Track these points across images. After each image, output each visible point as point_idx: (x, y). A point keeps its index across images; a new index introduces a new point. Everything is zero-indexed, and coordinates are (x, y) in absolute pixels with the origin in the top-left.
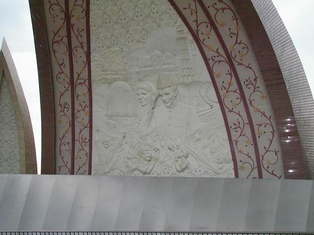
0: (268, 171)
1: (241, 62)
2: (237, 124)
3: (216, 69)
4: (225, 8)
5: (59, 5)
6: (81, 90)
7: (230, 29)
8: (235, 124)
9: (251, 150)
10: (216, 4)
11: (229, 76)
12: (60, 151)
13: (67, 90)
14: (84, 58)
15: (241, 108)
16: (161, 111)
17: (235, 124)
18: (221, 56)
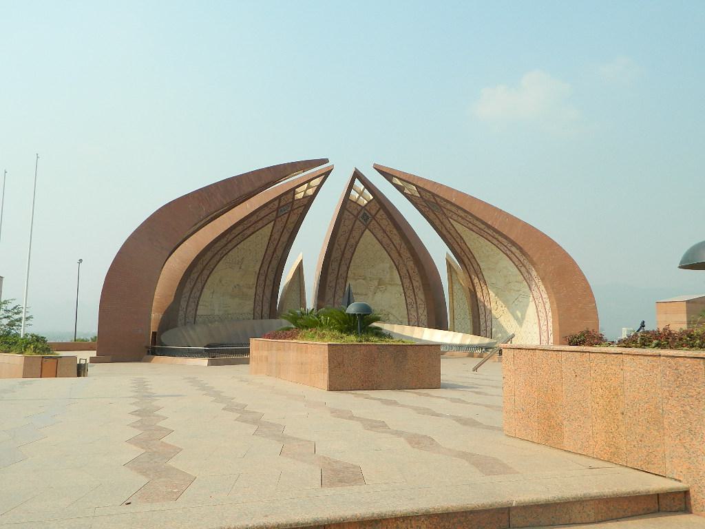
3: (404, 281)
6: (341, 281)
9: (415, 314)
14: (346, 269)
15: (413, 297)
16: (379, 295)
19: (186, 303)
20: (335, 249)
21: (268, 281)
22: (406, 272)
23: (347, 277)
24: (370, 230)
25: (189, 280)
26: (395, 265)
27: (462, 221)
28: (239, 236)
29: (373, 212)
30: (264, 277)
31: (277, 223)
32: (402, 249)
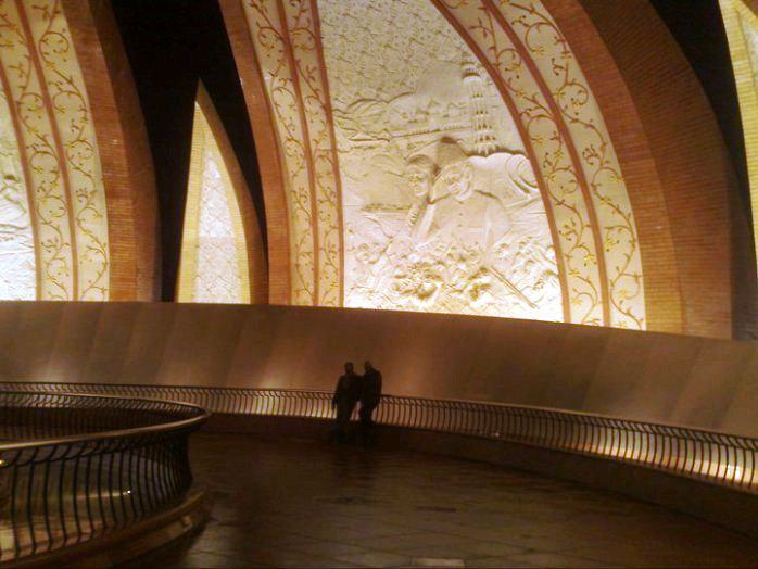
0: (620, 310)
1: (576, 117)
2: (571, 225)
4: (542, 23)
5: (272, 28)
6: (322, 167)
7: (553, 59)
8: (566, 226)
10: (524, 17)
11: (556, 142)
12: (297, 265)
13: (301, 168)
15: (576, 198)
17: (566, 226)
18: (542, 107)
20: (255, 30)
21: (73, 173)
22: (533, 89)
26: (485, 63)
30: (51, 162)
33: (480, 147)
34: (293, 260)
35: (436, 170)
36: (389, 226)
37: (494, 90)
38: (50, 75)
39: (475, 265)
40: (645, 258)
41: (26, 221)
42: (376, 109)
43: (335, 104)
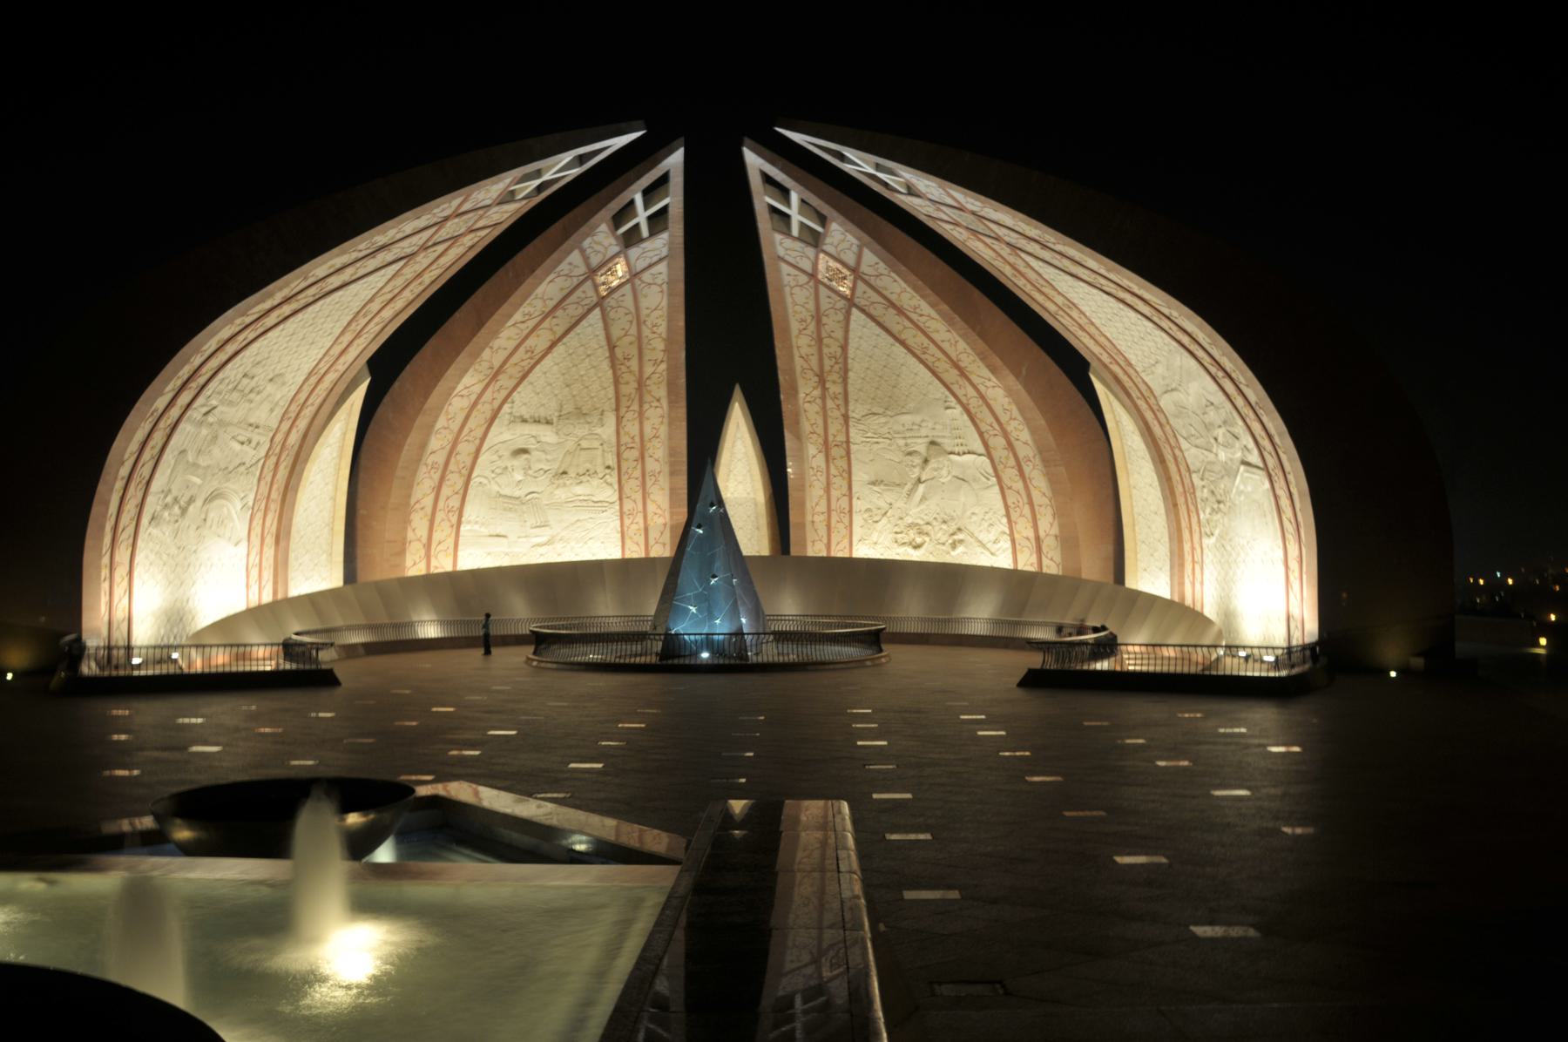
3: (991, 442)
15: (1019, 485)
19: (426, 524)
20: (798, 369)
21: (649, 461)
22: (991, 419)
23: (848, 442)
24: (863, 311)
25: (423, 469)
27: (1047, 255)
28: (522, 349)
29: (850, 258)
31: (612, 314)
32: (963, 357)
33: (957, 449)
34: (809, 518)
35: (926, 461)
36: (889, 496)
37: (965, 417)
38: (647, 398)
39: (954, 528)
40: (1061, 527)
41: (616, 497)
42: (883, 420)
43: (851, 414)
